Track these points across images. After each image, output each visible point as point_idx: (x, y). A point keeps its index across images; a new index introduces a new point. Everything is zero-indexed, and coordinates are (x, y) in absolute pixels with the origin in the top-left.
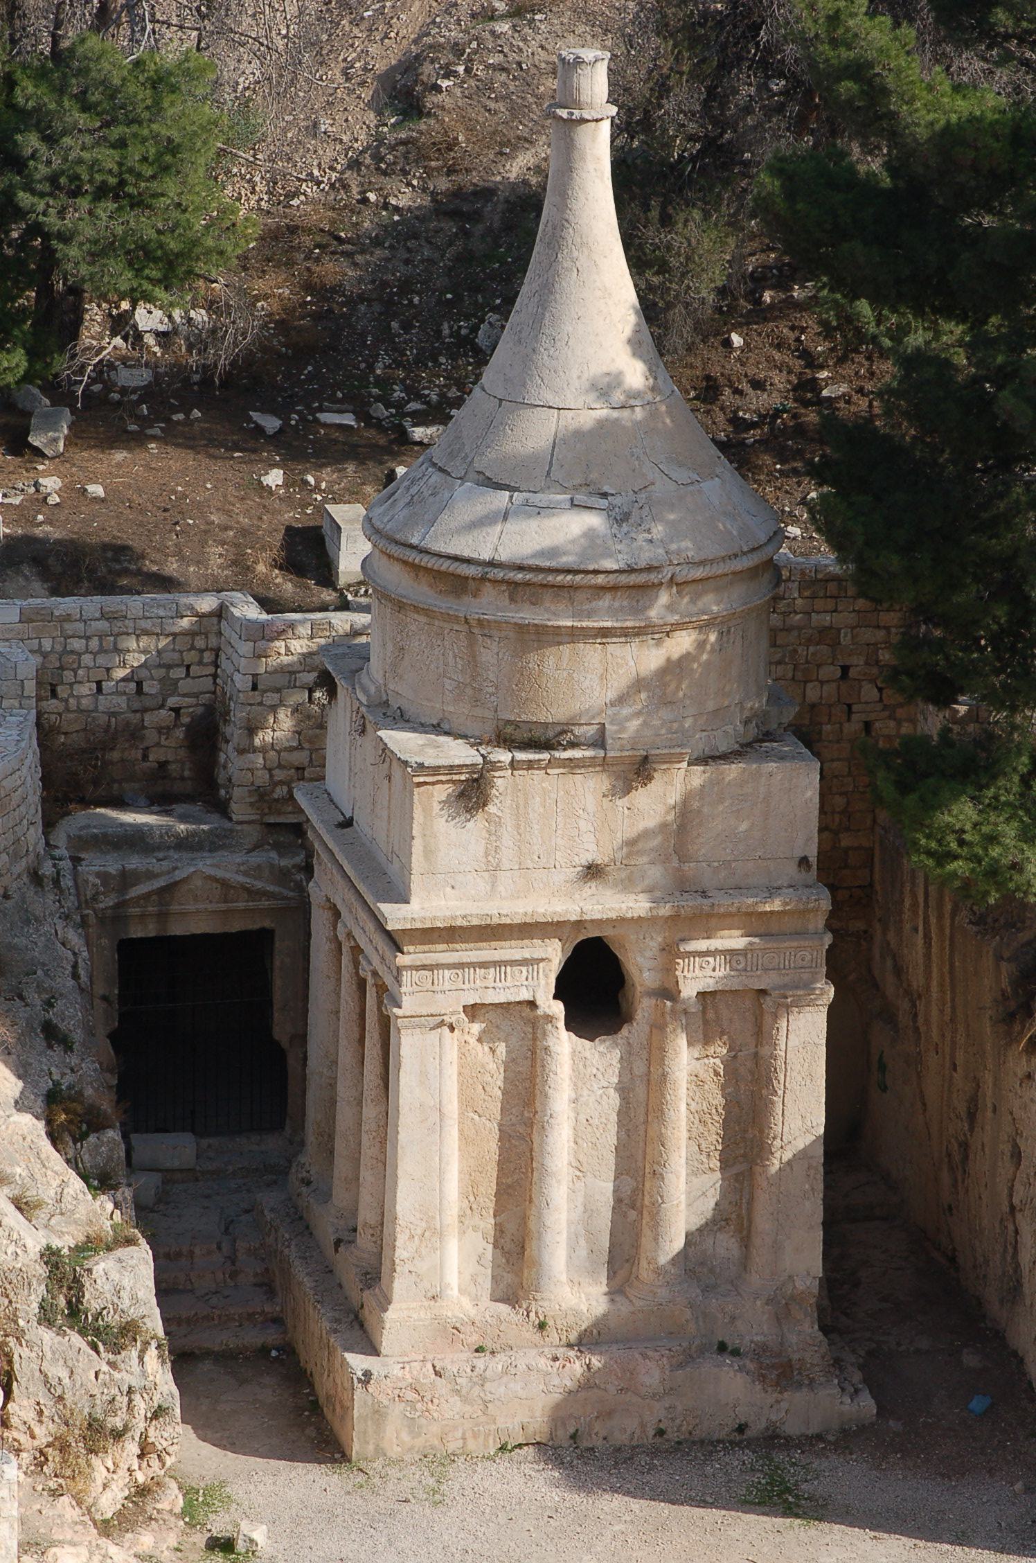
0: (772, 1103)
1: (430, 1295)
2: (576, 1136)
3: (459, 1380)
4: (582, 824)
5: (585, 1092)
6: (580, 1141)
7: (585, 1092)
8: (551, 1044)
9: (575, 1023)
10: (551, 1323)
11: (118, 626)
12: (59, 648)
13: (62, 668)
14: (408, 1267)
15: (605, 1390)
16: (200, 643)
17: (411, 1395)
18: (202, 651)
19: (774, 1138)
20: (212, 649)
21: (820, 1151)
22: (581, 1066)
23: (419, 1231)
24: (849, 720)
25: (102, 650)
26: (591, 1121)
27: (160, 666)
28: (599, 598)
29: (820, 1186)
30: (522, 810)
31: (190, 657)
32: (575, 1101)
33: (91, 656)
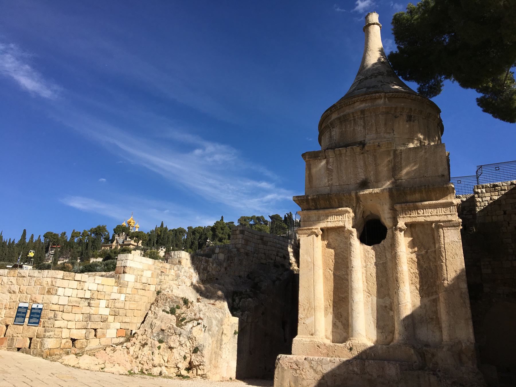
0: (442, 265)
1: (311, 333)
2: (367, 280)
3: (313, 362)
4: (359, 170)
5: (369, 264)
6: (368, 282)
7: (369, 264)
8: (351, 241)
9: (363, 240)
10: (354, 348)
14: (303, 321)
15: (372, 375)
17: (295, 367)
19: (444, 280)
21: (464, 286)
22: (367, 254)
23: (307, 308)
24: (509, 226)
26: (372, 275)
28: (362, 104)
29: (468, 301)
30: (339, 166)
32: (366, 267)
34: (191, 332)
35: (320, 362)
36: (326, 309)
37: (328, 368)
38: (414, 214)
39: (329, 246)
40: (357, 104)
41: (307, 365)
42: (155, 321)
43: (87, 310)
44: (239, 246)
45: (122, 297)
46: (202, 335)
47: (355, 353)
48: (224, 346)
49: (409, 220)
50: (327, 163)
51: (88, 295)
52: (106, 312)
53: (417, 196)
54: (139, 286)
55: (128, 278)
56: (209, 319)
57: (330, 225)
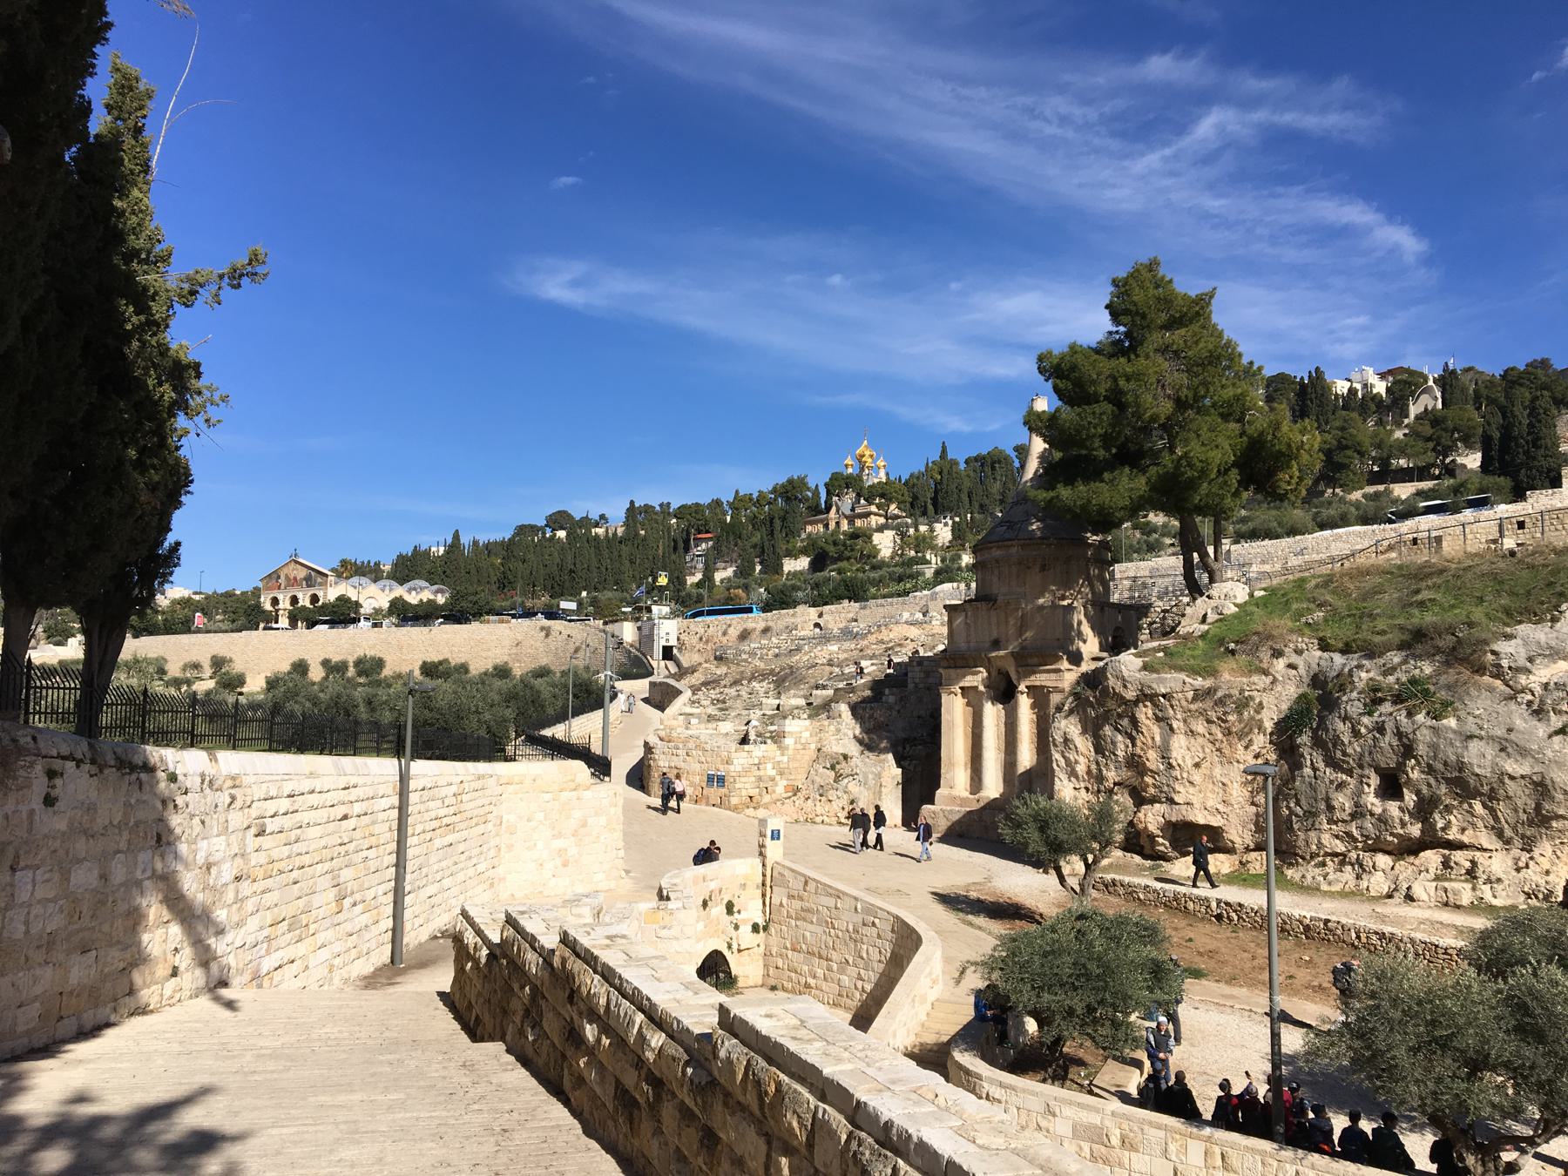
34: (846, 787)
35: (951, 812)
36: (966, 764)
37: (956, 817)
38: (1033, 678)
39: (968, 704)
40: (994, 549)
41: (941, 815)
42: (816, 778)
43: (758, 773)
44: (917, 681)
45: (785, 759)
46: (857, 789)
47: (982, 804)
48: (884, 797)
49: (1028, 683)
50: (966, 617)
51: (756, 761)
52: (772, 773)
53: (1035, 660)
54: (799, 746)
55: (789, 741)
56: (865, 774)
57: (967, 684)
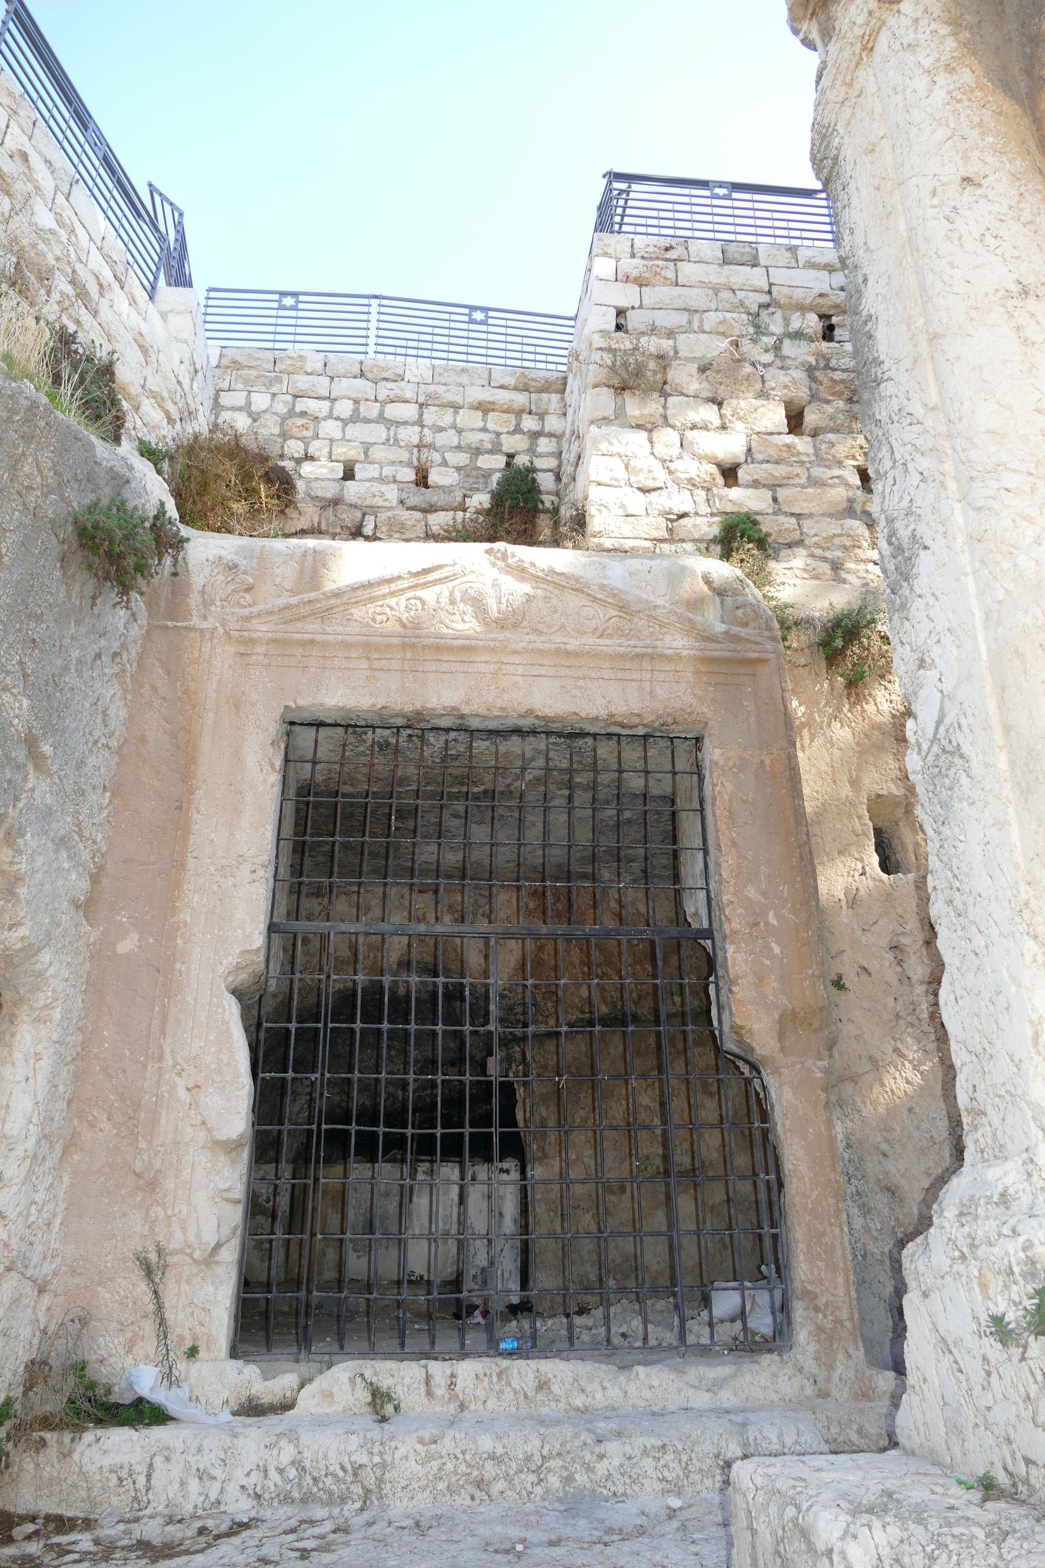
11: (384, 391)
12: (281, 408)
13: (285, 436)
16: (529, 423)
18: (535, 435)
20: (551, 435)
25: (355, 418)
27: (459, 448)
31: (510, 443)
33: (340, 424)
